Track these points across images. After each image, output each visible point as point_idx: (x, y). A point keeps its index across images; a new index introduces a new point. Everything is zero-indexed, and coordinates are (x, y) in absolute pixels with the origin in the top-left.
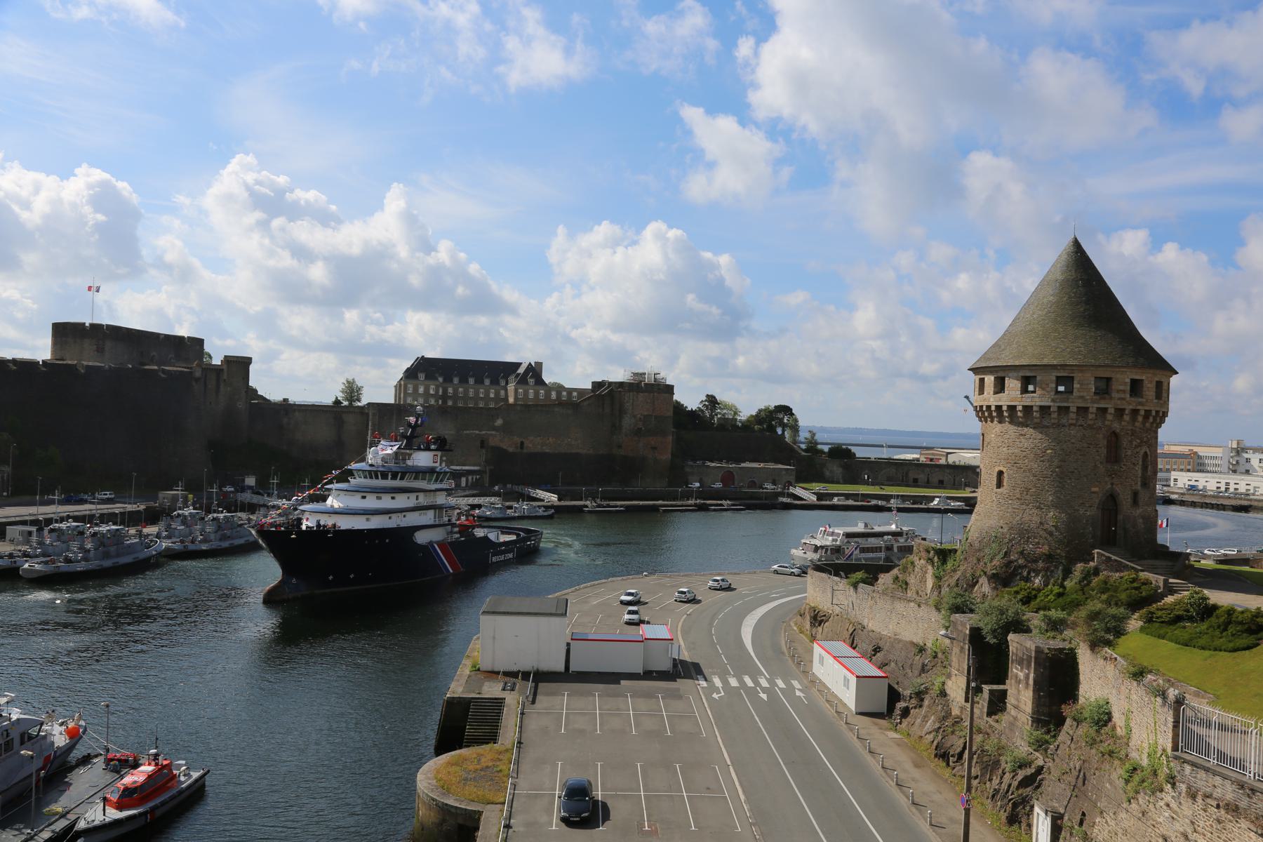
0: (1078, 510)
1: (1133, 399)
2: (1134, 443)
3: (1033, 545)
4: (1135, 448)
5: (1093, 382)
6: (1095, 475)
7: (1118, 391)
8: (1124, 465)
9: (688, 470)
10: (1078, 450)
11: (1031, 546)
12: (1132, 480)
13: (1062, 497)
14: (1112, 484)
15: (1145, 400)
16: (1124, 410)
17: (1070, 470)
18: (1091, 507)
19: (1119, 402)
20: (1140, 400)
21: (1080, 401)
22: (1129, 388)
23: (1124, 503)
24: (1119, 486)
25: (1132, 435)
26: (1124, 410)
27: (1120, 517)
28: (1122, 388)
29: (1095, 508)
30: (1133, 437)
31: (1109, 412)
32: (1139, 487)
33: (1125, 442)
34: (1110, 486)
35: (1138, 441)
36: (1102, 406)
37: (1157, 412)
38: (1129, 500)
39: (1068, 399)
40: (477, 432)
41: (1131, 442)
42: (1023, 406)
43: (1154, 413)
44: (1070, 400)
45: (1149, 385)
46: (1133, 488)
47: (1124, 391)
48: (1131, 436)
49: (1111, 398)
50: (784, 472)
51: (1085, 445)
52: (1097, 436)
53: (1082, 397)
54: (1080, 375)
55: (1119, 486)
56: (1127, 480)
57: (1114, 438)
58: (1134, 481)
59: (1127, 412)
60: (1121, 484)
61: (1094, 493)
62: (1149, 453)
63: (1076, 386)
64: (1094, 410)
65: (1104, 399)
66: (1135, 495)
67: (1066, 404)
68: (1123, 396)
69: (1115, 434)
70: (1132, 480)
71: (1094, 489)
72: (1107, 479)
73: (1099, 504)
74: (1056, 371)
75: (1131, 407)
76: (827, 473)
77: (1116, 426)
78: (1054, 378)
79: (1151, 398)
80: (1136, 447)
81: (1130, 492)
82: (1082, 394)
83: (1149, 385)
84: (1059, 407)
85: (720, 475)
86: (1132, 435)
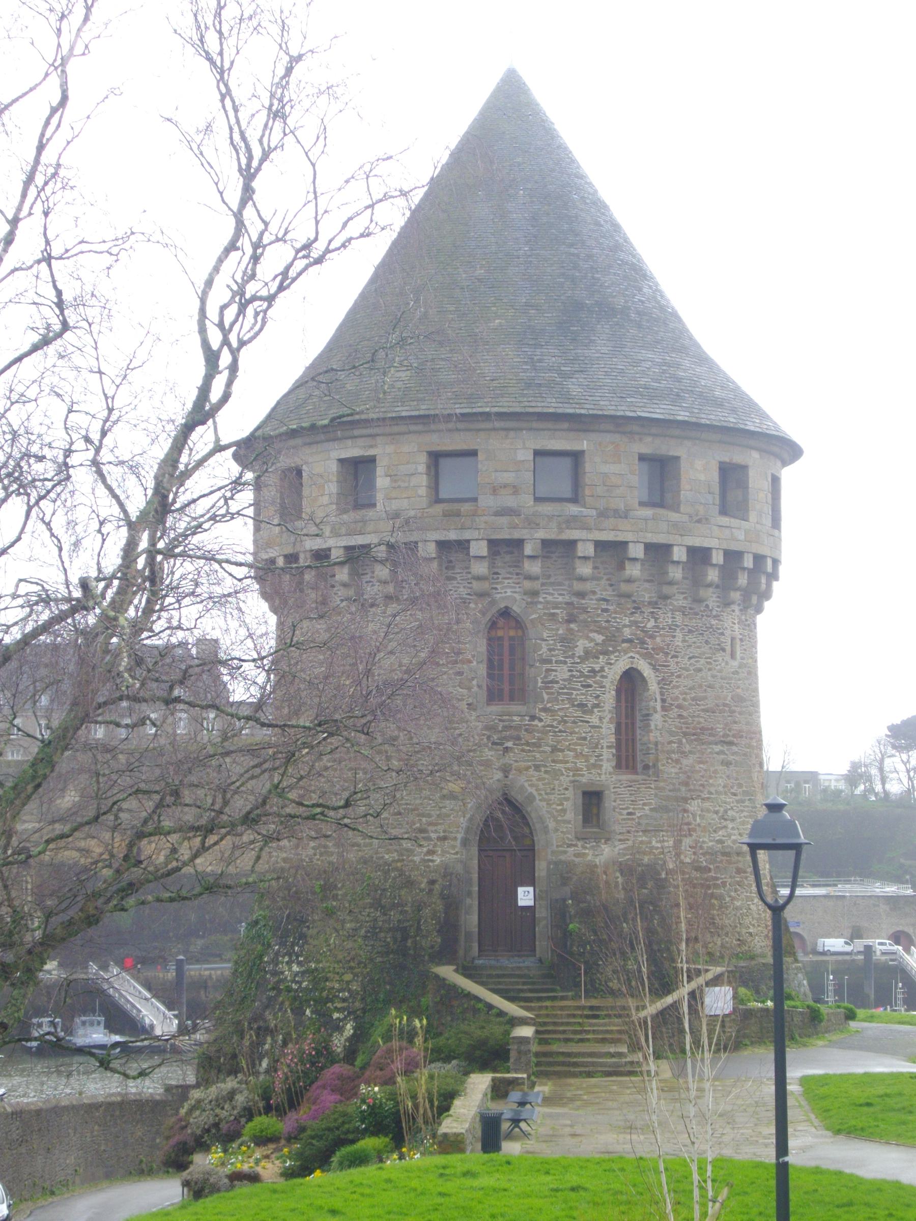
0: (410, 852)
2: (581, 645)
3: (300, 964)
5: (422, 468)
8: (545, 710)
11: (295, 968)
12: (578, 755)
14: (506, 770)
15: (594, 512)
16: (519, 543)
18: (445, 838)
19: (504, 520)
23: (551, 825)
24: (531, 772)
25: (571, 619)
28: (508, 477)
29: (458, 842)
30: (572, 626)
31: (473, 552)
34: (499, 775)
35: (599, 638)
36: (452, 536)
38: (570, 816)
39: (364, 521)
41: (567, 641)
44: (370, 527)
45: (605, 468)
48: (569, 621)
54: (390, 449)
55: (531, 772)
59: (528, 550)
60: (537, 768)
61: (452, 796)
63: (382, 482)
64: (432, 549)
67: (360, 540)
68: (510, 501)
70: (578, 755)
72: (488, 754)
73: (468, 830)
74: (336, 445)
75: (541, 534)
78: (334, 467)
80: (588, 655)
81: (570, 794)
82: (395, 505)
84: (348, 548)
86: (571, 619)
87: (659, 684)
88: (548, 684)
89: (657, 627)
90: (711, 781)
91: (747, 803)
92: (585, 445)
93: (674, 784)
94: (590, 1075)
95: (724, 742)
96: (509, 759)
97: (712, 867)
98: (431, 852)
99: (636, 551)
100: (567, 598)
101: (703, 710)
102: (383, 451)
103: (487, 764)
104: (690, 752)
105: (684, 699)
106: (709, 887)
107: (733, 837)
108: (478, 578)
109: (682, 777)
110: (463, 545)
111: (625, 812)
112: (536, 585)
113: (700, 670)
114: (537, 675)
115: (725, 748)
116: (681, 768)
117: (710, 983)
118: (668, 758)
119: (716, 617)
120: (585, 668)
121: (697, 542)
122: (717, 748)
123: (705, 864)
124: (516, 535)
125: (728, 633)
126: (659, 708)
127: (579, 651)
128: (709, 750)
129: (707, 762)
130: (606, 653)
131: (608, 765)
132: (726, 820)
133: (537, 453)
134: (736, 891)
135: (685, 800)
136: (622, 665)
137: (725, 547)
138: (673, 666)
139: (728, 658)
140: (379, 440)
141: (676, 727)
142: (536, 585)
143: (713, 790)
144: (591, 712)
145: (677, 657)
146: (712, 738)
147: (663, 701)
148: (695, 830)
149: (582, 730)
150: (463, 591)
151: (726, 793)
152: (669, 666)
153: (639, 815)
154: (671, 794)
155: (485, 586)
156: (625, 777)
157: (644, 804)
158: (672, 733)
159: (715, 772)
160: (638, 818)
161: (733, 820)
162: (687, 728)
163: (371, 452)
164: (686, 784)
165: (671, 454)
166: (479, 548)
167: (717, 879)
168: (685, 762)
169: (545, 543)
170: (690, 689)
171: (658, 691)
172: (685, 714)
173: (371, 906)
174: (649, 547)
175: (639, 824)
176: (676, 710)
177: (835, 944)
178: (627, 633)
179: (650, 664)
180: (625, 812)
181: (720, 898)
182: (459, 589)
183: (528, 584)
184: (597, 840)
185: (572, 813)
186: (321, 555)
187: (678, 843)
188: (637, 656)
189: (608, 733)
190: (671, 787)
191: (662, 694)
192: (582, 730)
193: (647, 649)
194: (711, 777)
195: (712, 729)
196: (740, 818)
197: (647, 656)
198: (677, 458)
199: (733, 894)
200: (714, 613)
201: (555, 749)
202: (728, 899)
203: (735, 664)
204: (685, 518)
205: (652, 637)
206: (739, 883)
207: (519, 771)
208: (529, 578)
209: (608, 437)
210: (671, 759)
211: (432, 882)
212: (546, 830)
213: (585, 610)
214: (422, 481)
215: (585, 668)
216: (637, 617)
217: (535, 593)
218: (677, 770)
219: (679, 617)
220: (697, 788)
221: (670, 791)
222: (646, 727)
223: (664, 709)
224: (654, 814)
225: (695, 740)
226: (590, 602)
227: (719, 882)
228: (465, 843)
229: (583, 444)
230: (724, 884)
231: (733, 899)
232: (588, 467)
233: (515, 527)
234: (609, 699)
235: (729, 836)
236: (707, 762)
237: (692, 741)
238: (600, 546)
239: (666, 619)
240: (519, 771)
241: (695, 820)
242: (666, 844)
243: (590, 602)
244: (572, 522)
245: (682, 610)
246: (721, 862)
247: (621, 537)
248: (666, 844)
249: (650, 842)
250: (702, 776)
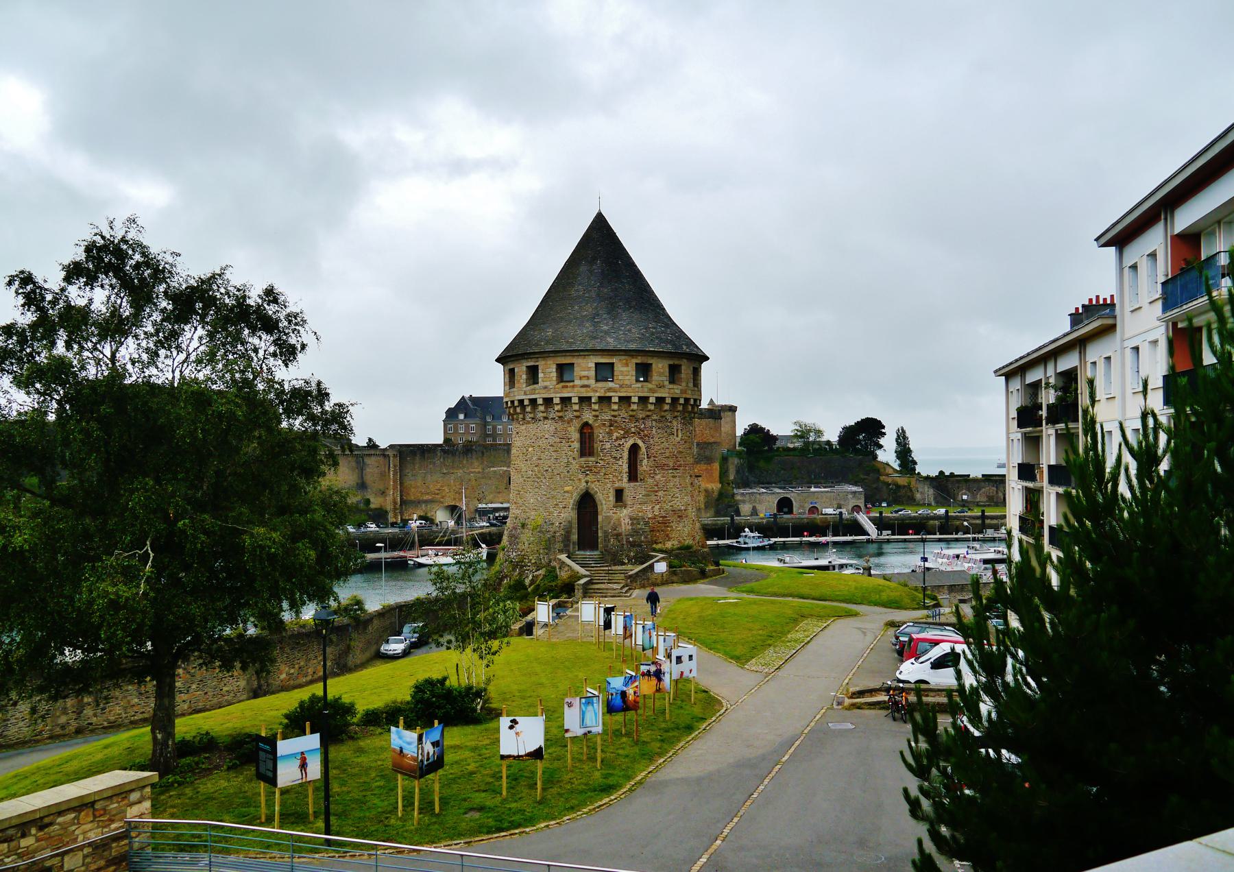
1: (600, 384)
2: (615, 435)
4: (616, 440)
5: (554, 370)
6: (568, 472)
7: (581, 378)
9: (738, 498)
10: (551, 446)
13: (539, 498)
14: (587, 482)
15: (617, 386)
16: (590, 398)
17: (545, 469)
19: (583, 390)
20: (611, 385)
21: (544, 391)
22: (592, 373)
23: (604, 502)
25: (611, 425)
26: (590, 398)
27: (600, 518)
32: (624, 483)
33: (600, 433)
35: (622, 432)
37: (687, 400)
40: (505, 469)
41: (610, 433)
42: (529, 399)
43: (682, 401)
44: (537, 392)
46: (616, 485)
47: (588, 378)
48: (610, 426)
49: (573, 386)
50: (850, 496)
51: (558, 440)
52: (569, 429)
53: (545, 387)
54: (543, 362)
56: (607, 477)
57: (586, 432)
58: (617, 477)
59: (593, 400)
61: (567, 492)
62: (640, 443)
63: (541, 375)
65: (567, 387)
66: (619, 494)
68: (586, 382)
69: (586, 424)
71: (567, 488)
72: (580, 476)
75: (598, 394)
76: (918, 496)
77: (588, 416)
78: (524, 369)
79: (627, 382)
80: (617, 439)
81: (611, 490)
82: (546, 384)
83: (625, 369)
85: (776, 502)
86: (611, 425)
88: (602, 450)
92: (614, 360)
94: (606, 597)
96: (588, 478)
98: (559, 513)
99: (635, 399)
100: (610, 418)
102: (541, 364)
103: (580, 479)
108: (575, 411)
110: (570, 399)
112: (597, 413)
114: (597, 446)
117: (657, 561)
119: (670, 422)
120: (616, 444)
121: (659, 395)
122: (671, 471)
124: (589, 395)
125: (675, 428)
127: (614, 437)
130: (624, 438)
131: (625, 479)
133: (597, 364)
135: (657, 491)
136: (631, 442)
138: (652, 442)
139: (675, 437)
140: (540, 359)
142: (597, 413)
144: (619, 460)
149: (615, 467)
150: (571, 416)
155: (578, 414)
156: (632, 484)
163: (537, 364)
166: (575, 400)
169: (599, 397)
173: (539, 532)
174: (640, 398)
177: (830, 511)
178: (633, 430)
181: (672, 527)
182: (569, 415)
183: (594, 413)
184: (621, 507)
185: (612, 498)
186: (521, 402)
189: (625, 467)
192: (615, 467)
197: (641, 438)
198: (651, 364)
201: (605, 474)
203: (679, 439)
204: (655, 387)
205: (643, 431)
207: (592, 482)
208: (595, 410)
209: (623, 357)
211: (560, 523)
212: (602, 504)
213: (616, 422)
214: (554, 374)
215: (616, 444)
216: (637, 424)
217: (597, 416)
219: (654, 423)
222: (641, 466)
223: (648, 458)
226: (618, 419)
228: (572, 509)
229: (614, 360)
232: (615, 368)
233: (588, 392)
234: (626, 455)
238: (620, 398)
239: (649, 423)
240: (592, 482)
243: (618, 419)
244: (610, 390)
245: (655, 420)
247: (629, 395)
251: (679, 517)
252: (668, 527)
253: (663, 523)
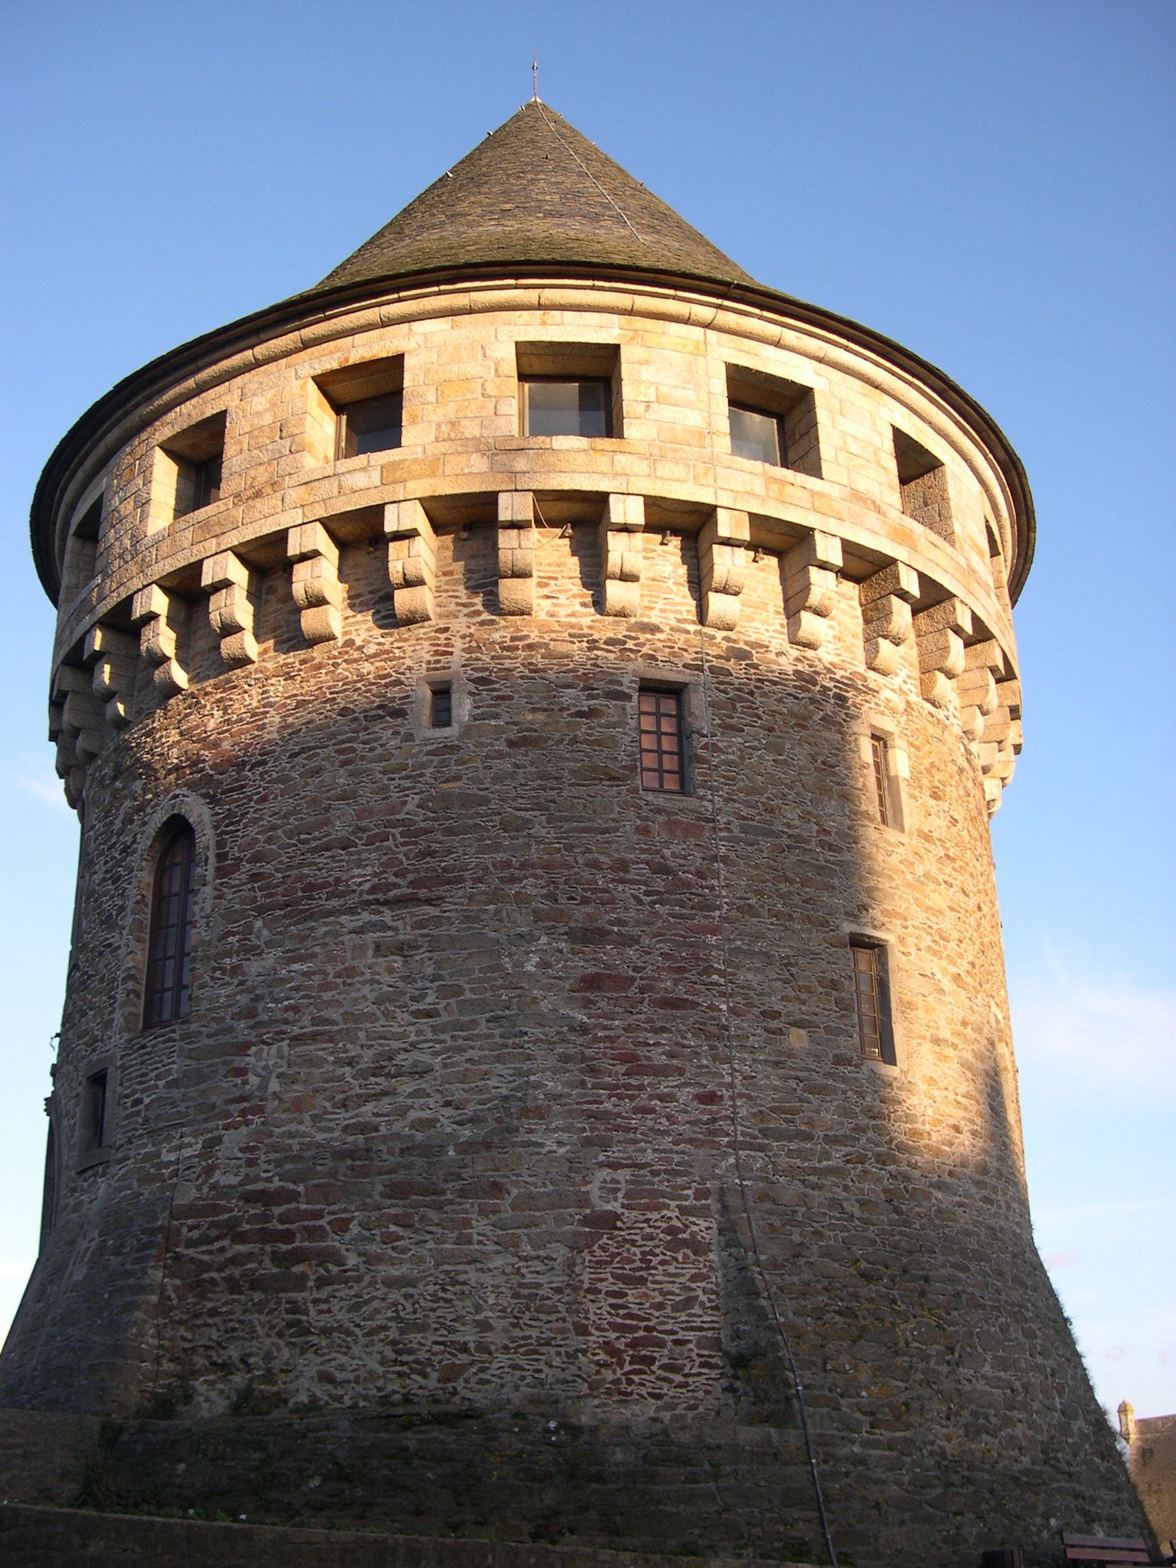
87: (216, 828)
89: (228, 721)
90: (326, 996)
91: (483, 1028)
93: (222, 1020)
95: (378, 902)
97: (301, 1188)
101: (315, 850)
104: (269, 944)
105: (269, 840)
106: (288, 1236)
107: (413, 1115)
109: (243, 999)
111: (129, 1101)
113: (318, 771)
115: (388, 916)
116: (241, 983)
118: (214, 970)
123: (277, 1183)
126: (210, 874)
128: (324, 929)
129: (314, 955)
132: (389, 1075)
134: (388, 1239)
135: (243, 1048)
137: (322, 513)
141: (242, 902)
143: (334, 1014)
145: (264, 763)
146: (335, 903)
147: (221, 857)
148: (259, 1110)
151: (388, 1014)
152: (244, 786)
153: (147, 1101)
154: (211, 1041)
157: (158, 1078)
158: (229, 916)
159: (351, 972)
160: (147, 1107)
161: (420, 1072)
162: (268, 896)
164: (250, 1013)
165: (209, 413)
167: (318, 1215)
168: (254, 967)
170: (285, 816)
171: (212, 844)
172: (268, 868)
175: (147, 1120)
176: (248, 866)
179: (205, 796)
180: (129, 1101)
181: (325, 1257)
187: (213, 1143)
188: (185, 791)
190: (214, 1026)
191: (220, 844)
193: (203, 770)
194: (327, 987)
195: (338, 881)
196: (445, 1066)
199: (374, 1248)
200: (371, 649)
202: (352, 1260)
206: (396, 1221)
210: (224, 971)
218: (230, 990)
220: (279, 1016)
221: (209, 1036)
223: (222, 872)
224: (176, 1093)
225: (284, 917)
227: (323, 1222)
230: (341, 1226)
231: (372, 1260)
235: (403, 1112)
236: (314, 955)
237: (276, 920)
241: (263, 1087)
242: (188, 1152)
246: (334, 1174)
248: (188, 1152)
249: (158, 1155)
250: (296, 989)
251: (397, 1191)
252: (299, 1256)
253: (267, 1236)
